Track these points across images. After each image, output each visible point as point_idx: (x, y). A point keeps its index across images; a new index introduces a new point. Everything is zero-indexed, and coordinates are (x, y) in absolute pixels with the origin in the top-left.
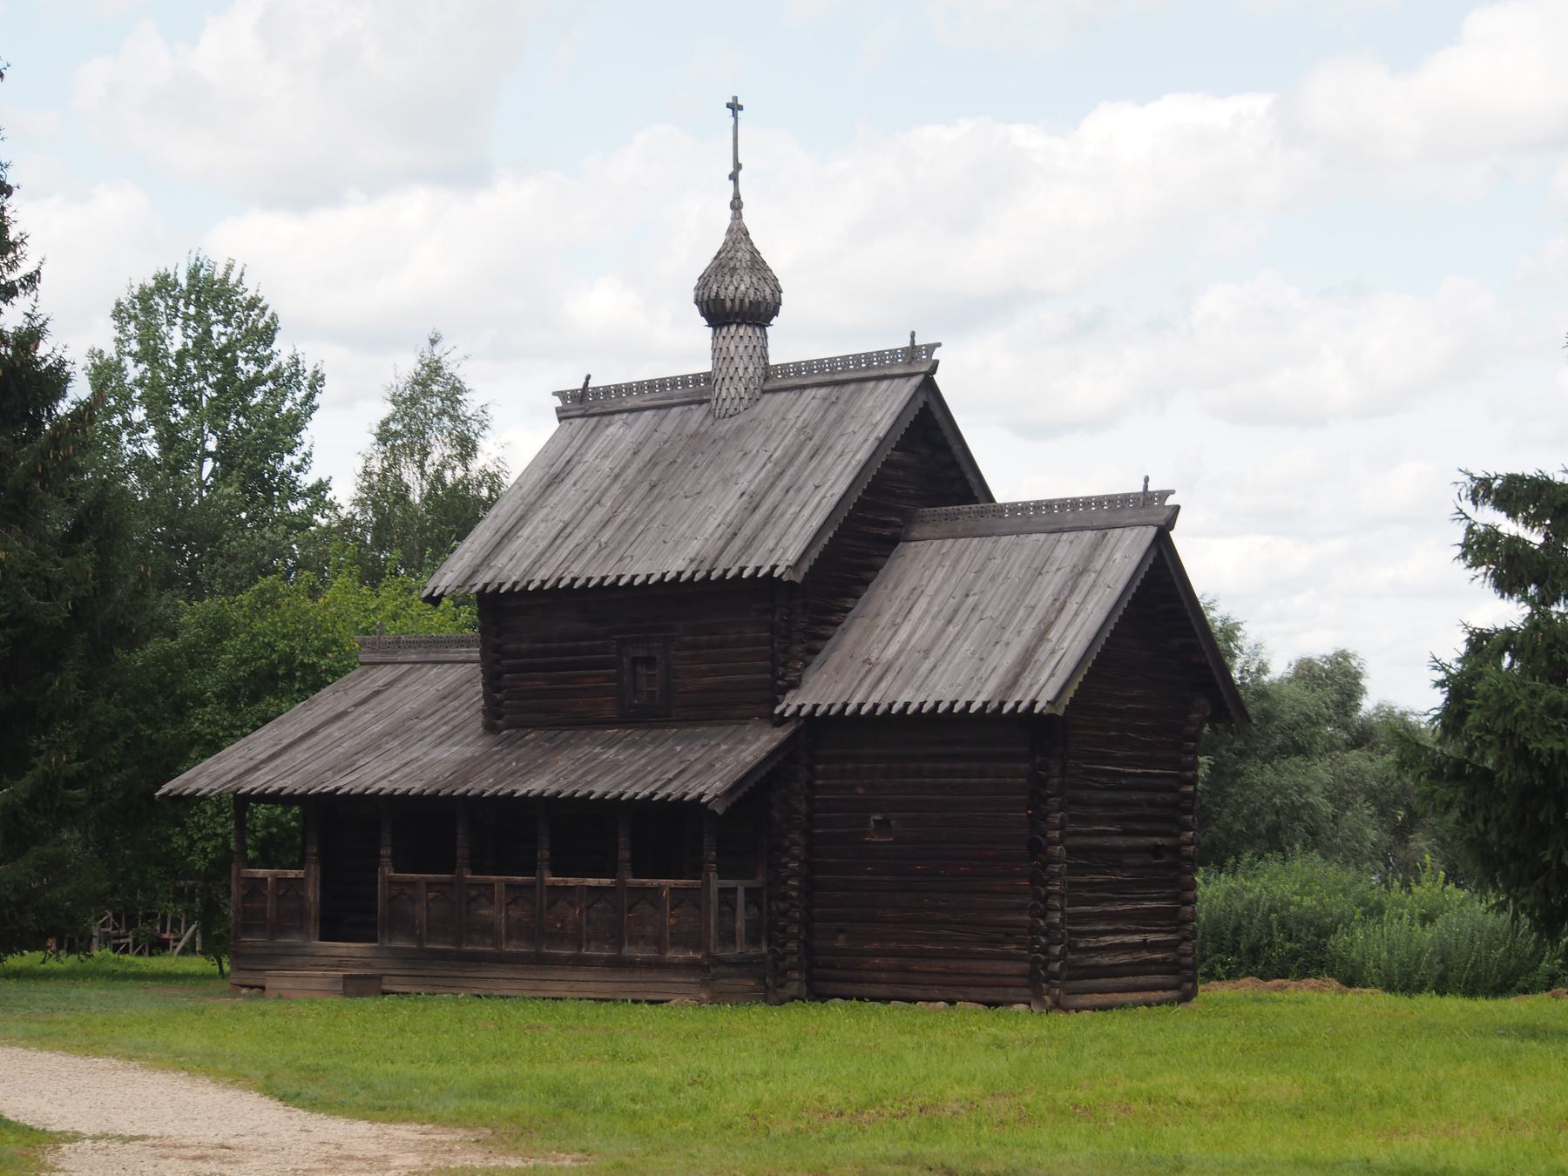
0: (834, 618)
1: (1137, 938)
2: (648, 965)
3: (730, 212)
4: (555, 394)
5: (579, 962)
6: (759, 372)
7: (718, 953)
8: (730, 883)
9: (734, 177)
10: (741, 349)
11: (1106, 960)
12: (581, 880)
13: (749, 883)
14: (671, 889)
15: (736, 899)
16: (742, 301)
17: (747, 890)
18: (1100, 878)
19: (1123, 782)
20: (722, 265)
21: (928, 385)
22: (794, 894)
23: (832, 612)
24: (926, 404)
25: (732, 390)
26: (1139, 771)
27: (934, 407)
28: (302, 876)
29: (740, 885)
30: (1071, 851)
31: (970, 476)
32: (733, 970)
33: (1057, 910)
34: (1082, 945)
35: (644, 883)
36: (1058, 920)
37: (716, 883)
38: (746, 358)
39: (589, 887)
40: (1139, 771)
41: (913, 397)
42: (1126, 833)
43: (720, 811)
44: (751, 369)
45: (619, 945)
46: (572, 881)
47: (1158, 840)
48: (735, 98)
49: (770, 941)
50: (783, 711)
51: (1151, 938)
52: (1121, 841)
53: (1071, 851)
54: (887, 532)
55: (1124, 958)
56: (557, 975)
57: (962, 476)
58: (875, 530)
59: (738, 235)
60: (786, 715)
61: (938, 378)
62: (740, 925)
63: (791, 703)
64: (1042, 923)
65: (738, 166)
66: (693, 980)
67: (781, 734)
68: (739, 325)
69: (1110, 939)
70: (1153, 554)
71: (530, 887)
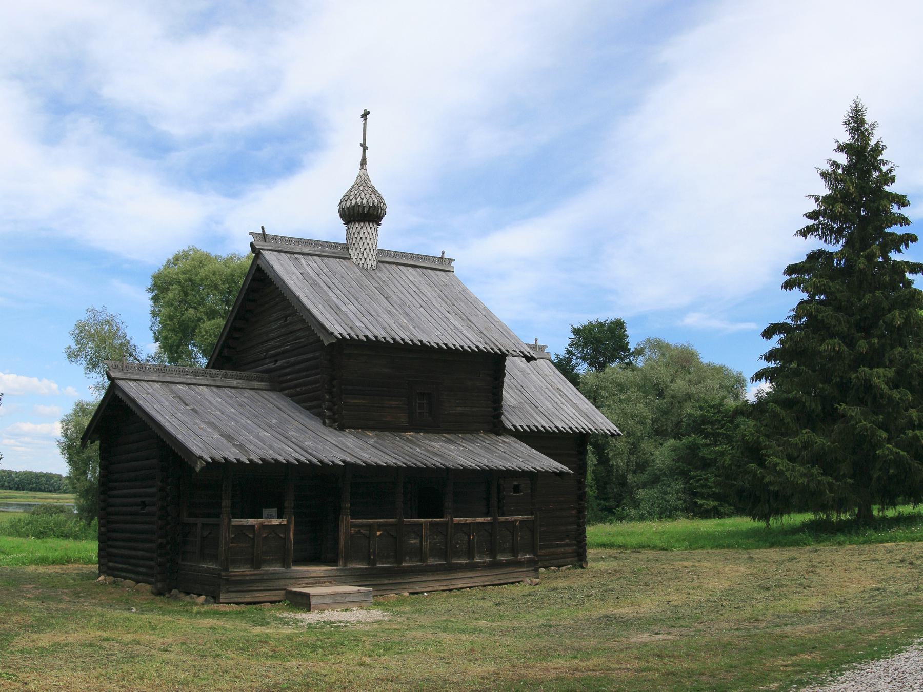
2: (508, 564)
4: (251, 233)
5: (472, 567)
12: (474, 519)
14: (520, 521)
28: (285, 523)
35: (507, 519)
39: (480, 523)
46: (469, 520)
56: (460, 575)
66: (530, 569)
71: (445, 524)
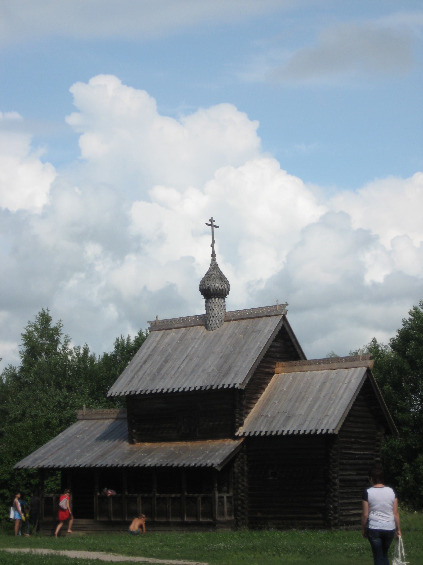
0: (254, 401)
3: (211, 258)
4: (148, 322)
6: (223, 314)
8: (222, 495)
9: (212, 246)
10: (216, 306)
11: (352, 519)
13: (228, 495)
15: (224, 501)
16: (216, 290)
17: (227, 497)
18: (350, 490)
19: (357, 457)
20: (208, 276)
21: (284, 318)
22: (243, 498)
24: (283, 325)
25: (213, 321)
26: (361, 453)
27: (286, 327)
29: (225, 496)
30: (341, 481)
31: (298, 350)
34: (344, 514)
36: (337, 505)
38: (218, 310)
40: (361, 453)
41: (279, 323)
42: (358, 474)
43: (219, 469)
44: (220, 313)
45: (183, 517)
48: (212, 218)
50: (238, 435)
52: (356, 477)
54: (270, 371)
57: (295, 350)
58: (267, 370)
59: (214, 267)
60: (240, 436)
61: (288, 317)
62: (226, 510)
63: (240, 431)
64: (331, 506)
65: (213, 242)
67: (237, 443)
68: (215, 298)
69: (353, 512)
70: (366, 377)
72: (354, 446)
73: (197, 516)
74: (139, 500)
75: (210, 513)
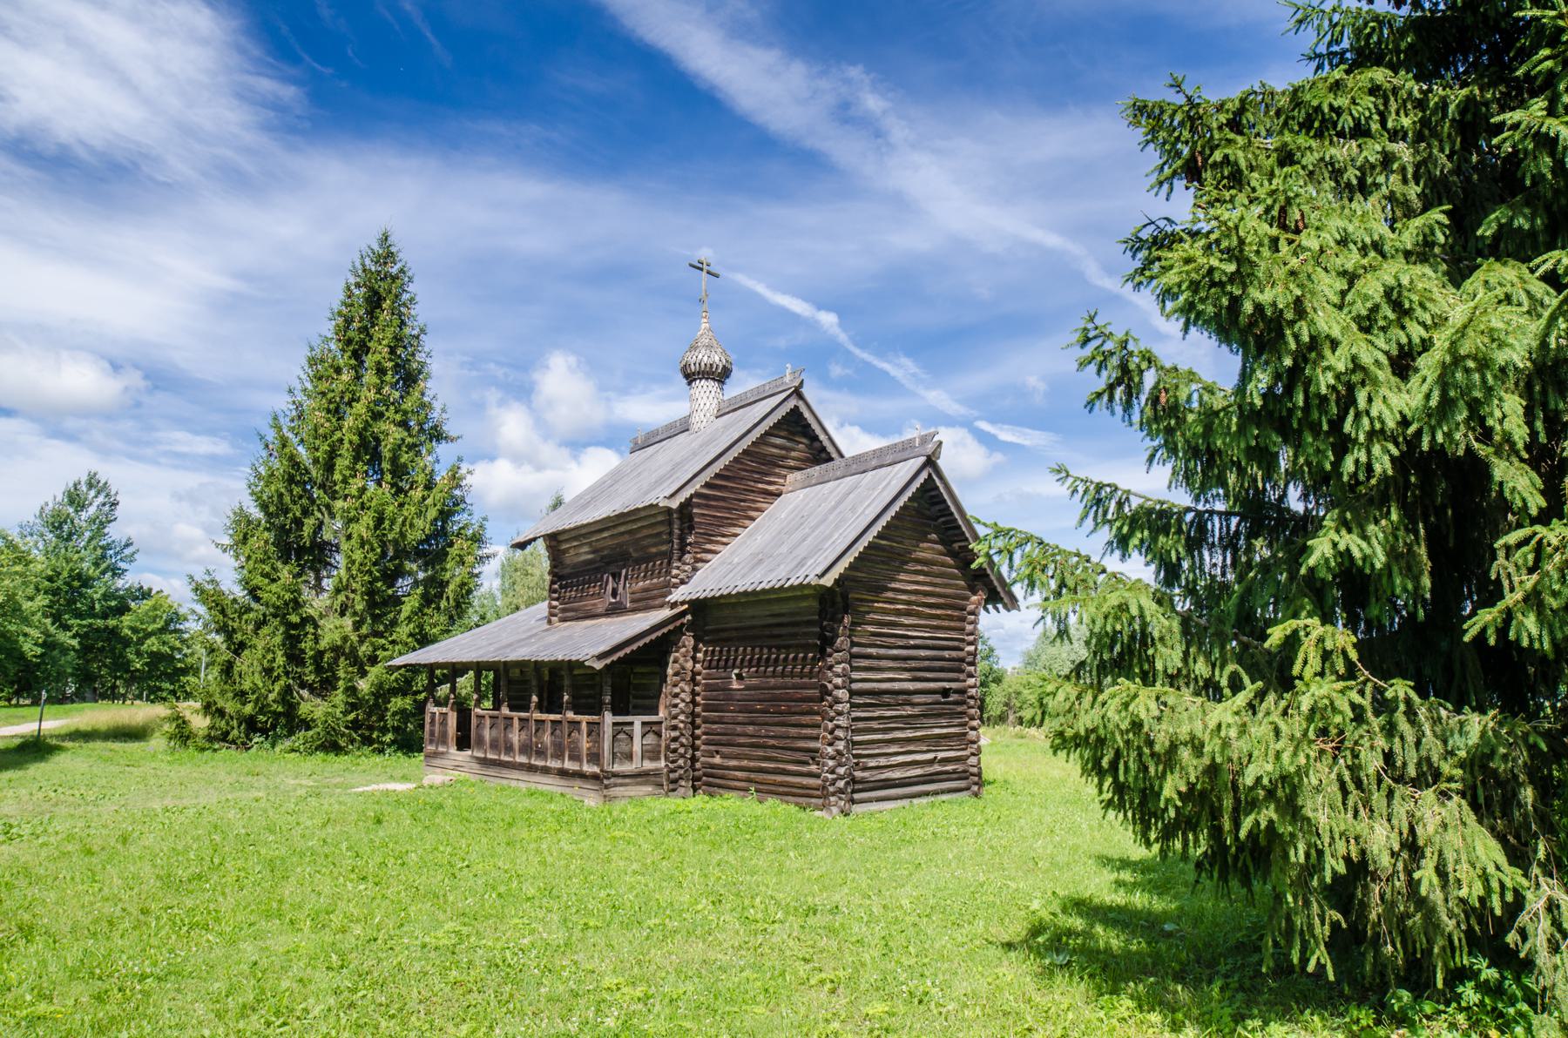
0: (724, 540)
1: (930, 756)
7: (617, 768)
17: (644, 724)
23: (724, 536)
24: (796, 407)
32: (627, 781)
33: (841, 739)
37: (609, 718)
47: (947, 685)
49: (666, 758)
51: (941, 755)
53: (852, 693)
54: (771, 488)
55: (919, 772)
62: (637, 748)
69: (901, 759)
70: (924, 475)
72: (906, 621)
73: (575, 757)
74: (516, 722)
75: (595, 757)
